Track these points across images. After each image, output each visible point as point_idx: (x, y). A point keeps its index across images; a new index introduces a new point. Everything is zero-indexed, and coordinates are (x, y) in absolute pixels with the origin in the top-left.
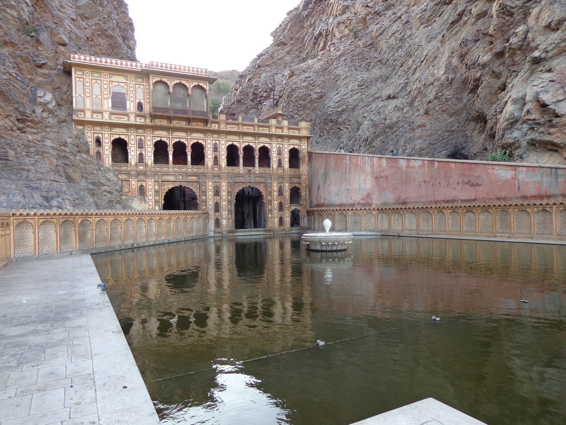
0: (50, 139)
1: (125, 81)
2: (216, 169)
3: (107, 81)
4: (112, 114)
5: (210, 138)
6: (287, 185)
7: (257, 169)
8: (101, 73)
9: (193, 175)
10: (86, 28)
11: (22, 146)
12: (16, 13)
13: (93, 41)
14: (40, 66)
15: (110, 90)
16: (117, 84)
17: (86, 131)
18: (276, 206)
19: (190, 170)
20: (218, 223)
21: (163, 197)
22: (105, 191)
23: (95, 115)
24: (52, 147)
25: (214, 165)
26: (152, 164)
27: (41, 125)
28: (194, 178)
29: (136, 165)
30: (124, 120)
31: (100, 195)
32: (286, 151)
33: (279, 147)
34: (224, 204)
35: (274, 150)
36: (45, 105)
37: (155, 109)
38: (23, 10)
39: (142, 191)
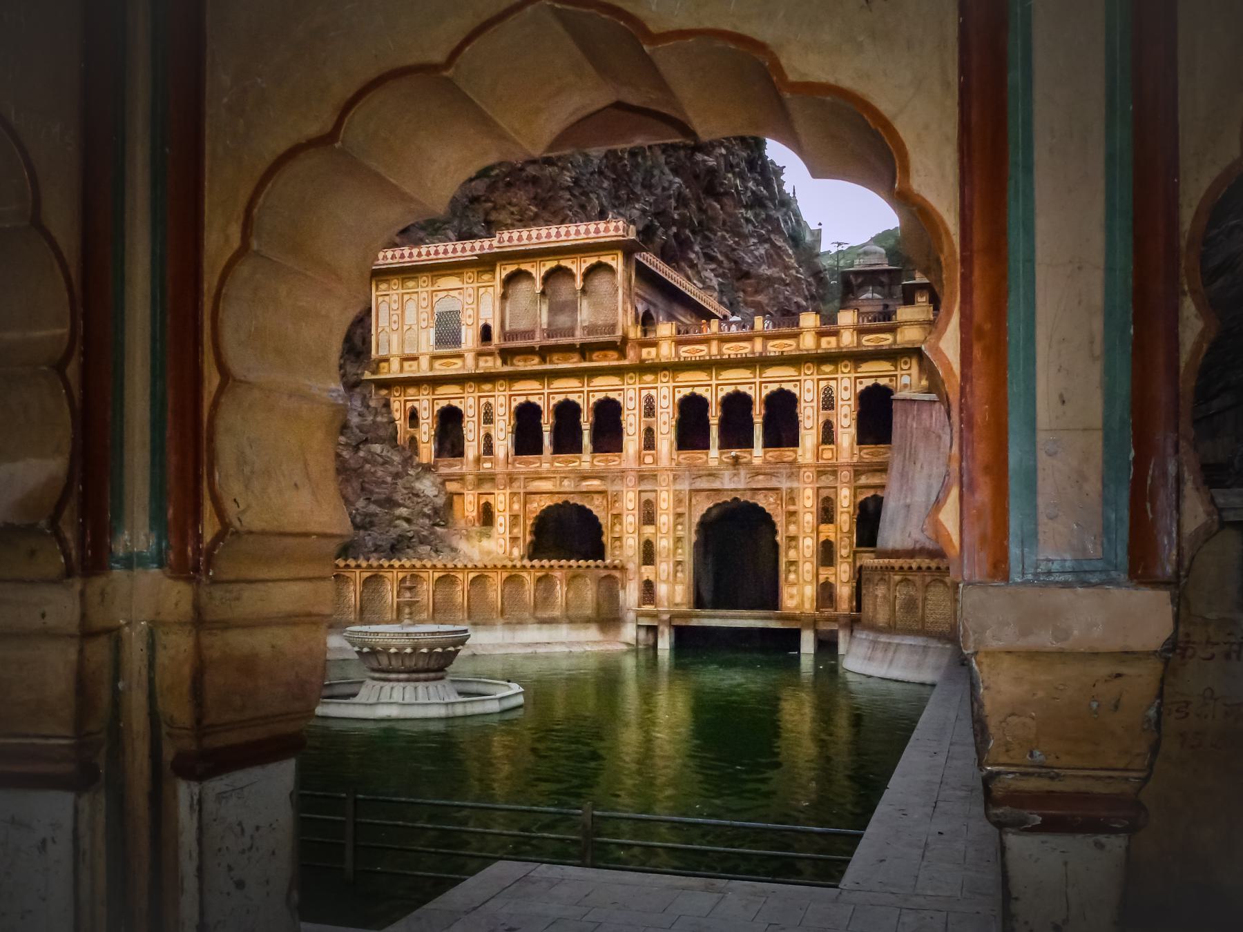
1: (459, 285)
2: (649, 460)
4: (435, 358)
5: (634, 383)
7: (758, 453)
8: (417, 278)
15: (433, 308)
16: (445, 293)
17: (392, 399)
18: (808, 553)
19: (586, 466)
20: (648, 589)
21: (528, 528)
22: (399, 518)
23: (406, 364)
29: (478, 460)
33: (828, 388)
34: (663, 544)
37: (506, 336)
39: (487, 516)
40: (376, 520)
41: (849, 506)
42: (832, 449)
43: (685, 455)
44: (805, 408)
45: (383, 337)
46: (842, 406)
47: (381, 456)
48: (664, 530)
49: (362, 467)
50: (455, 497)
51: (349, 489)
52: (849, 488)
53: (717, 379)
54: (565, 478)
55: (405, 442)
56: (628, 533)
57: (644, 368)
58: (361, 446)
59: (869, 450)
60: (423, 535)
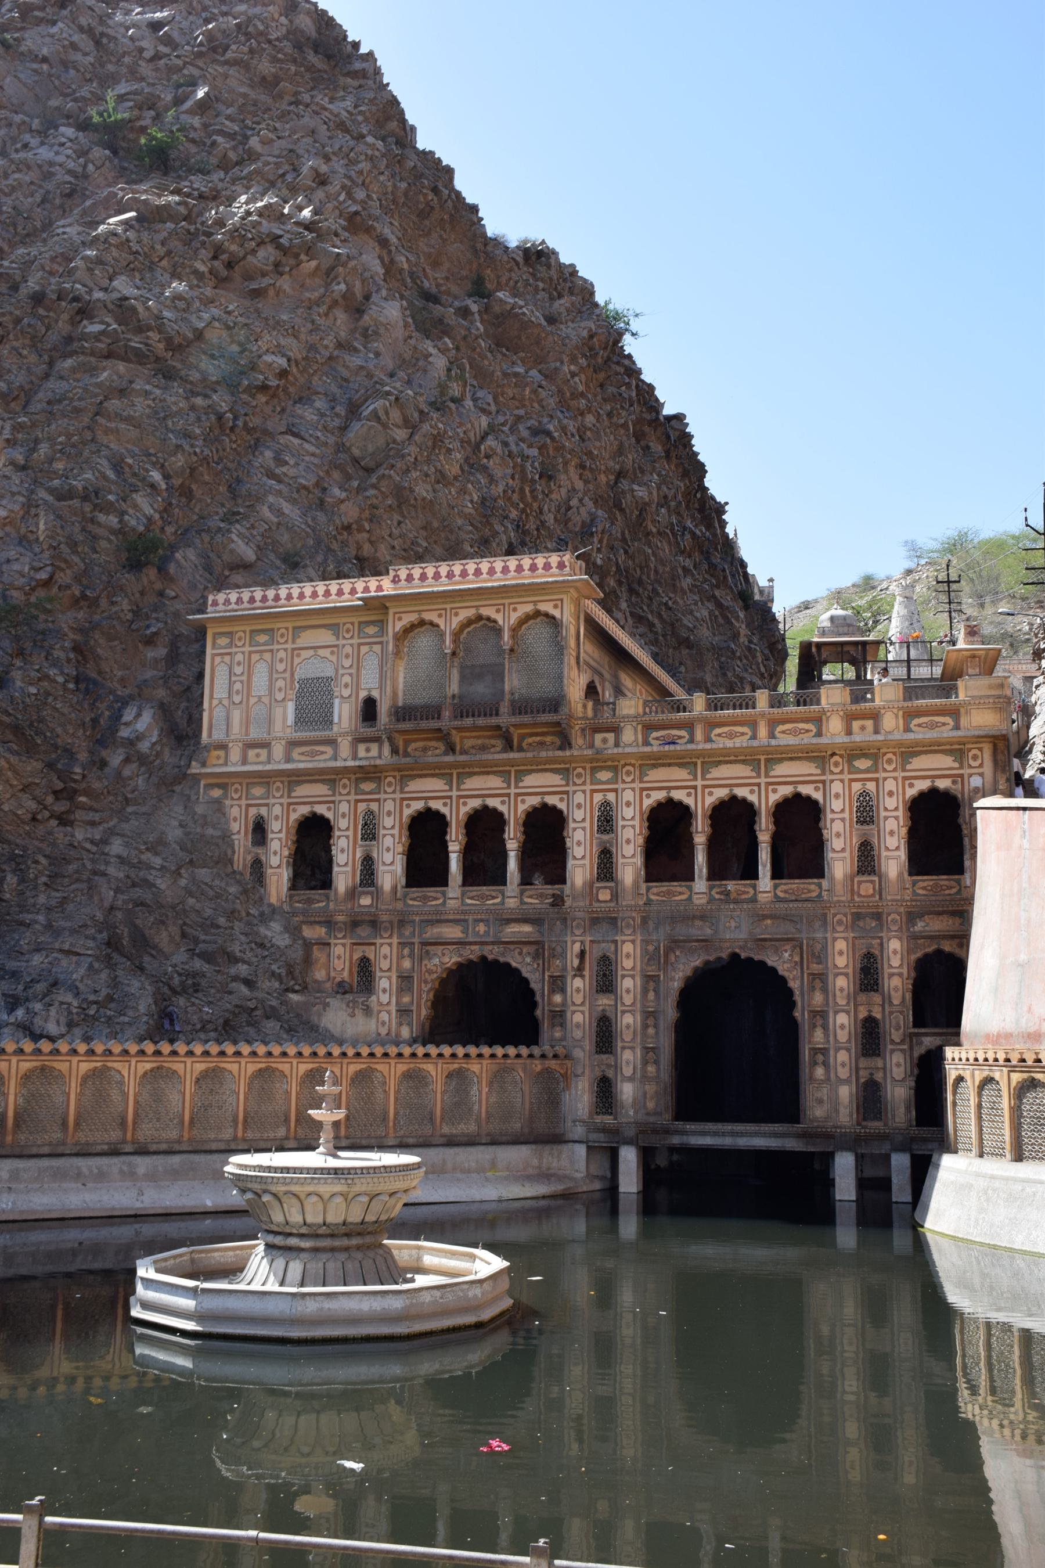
0: (123, 835)
3: (286, 650)
4: (293, 744)
6: (895, 945)
9: (525, 920)
10: (342, 501)
11: (44, 861)
12: (116, 520)
13: (365, 531)
14: (150, 641)
15: (292, 675)
16: (311, 652)
17: (228, 802)
18: (843, 1036)
19: (512, 903)
22: (235, 979)
23: (252, 753)
24: (119, 857)
25: (599, 879)
26: (394, 889)
27: (111, 798)
28: (527, 928)
29: (352, 894)
30: (324, 759)
31: (213, 991)
32: (891, 807)
33: (864, 794)
34: (628, 1021)
35: (837, 805)
36: (131, 743)
38: (135, 506)
40: (204, 983)
41: (901, 966)
42: (873, 882)
43: (658, 888)
44: (833, 820)
45: (219, 713)
46: (886, 818)
47: (211, 887)
48: (628, 1000)
49: (182, 902)
50: (317, 953)
51: (165, 934)
52: (900, 939)
53: (703, 779)
54: (482, 920)
55: (245, 865)
56: (574, 1004)
57: (598, 763)
58: (183, 871)
59: (925, 884)
60: (271, 1007)
